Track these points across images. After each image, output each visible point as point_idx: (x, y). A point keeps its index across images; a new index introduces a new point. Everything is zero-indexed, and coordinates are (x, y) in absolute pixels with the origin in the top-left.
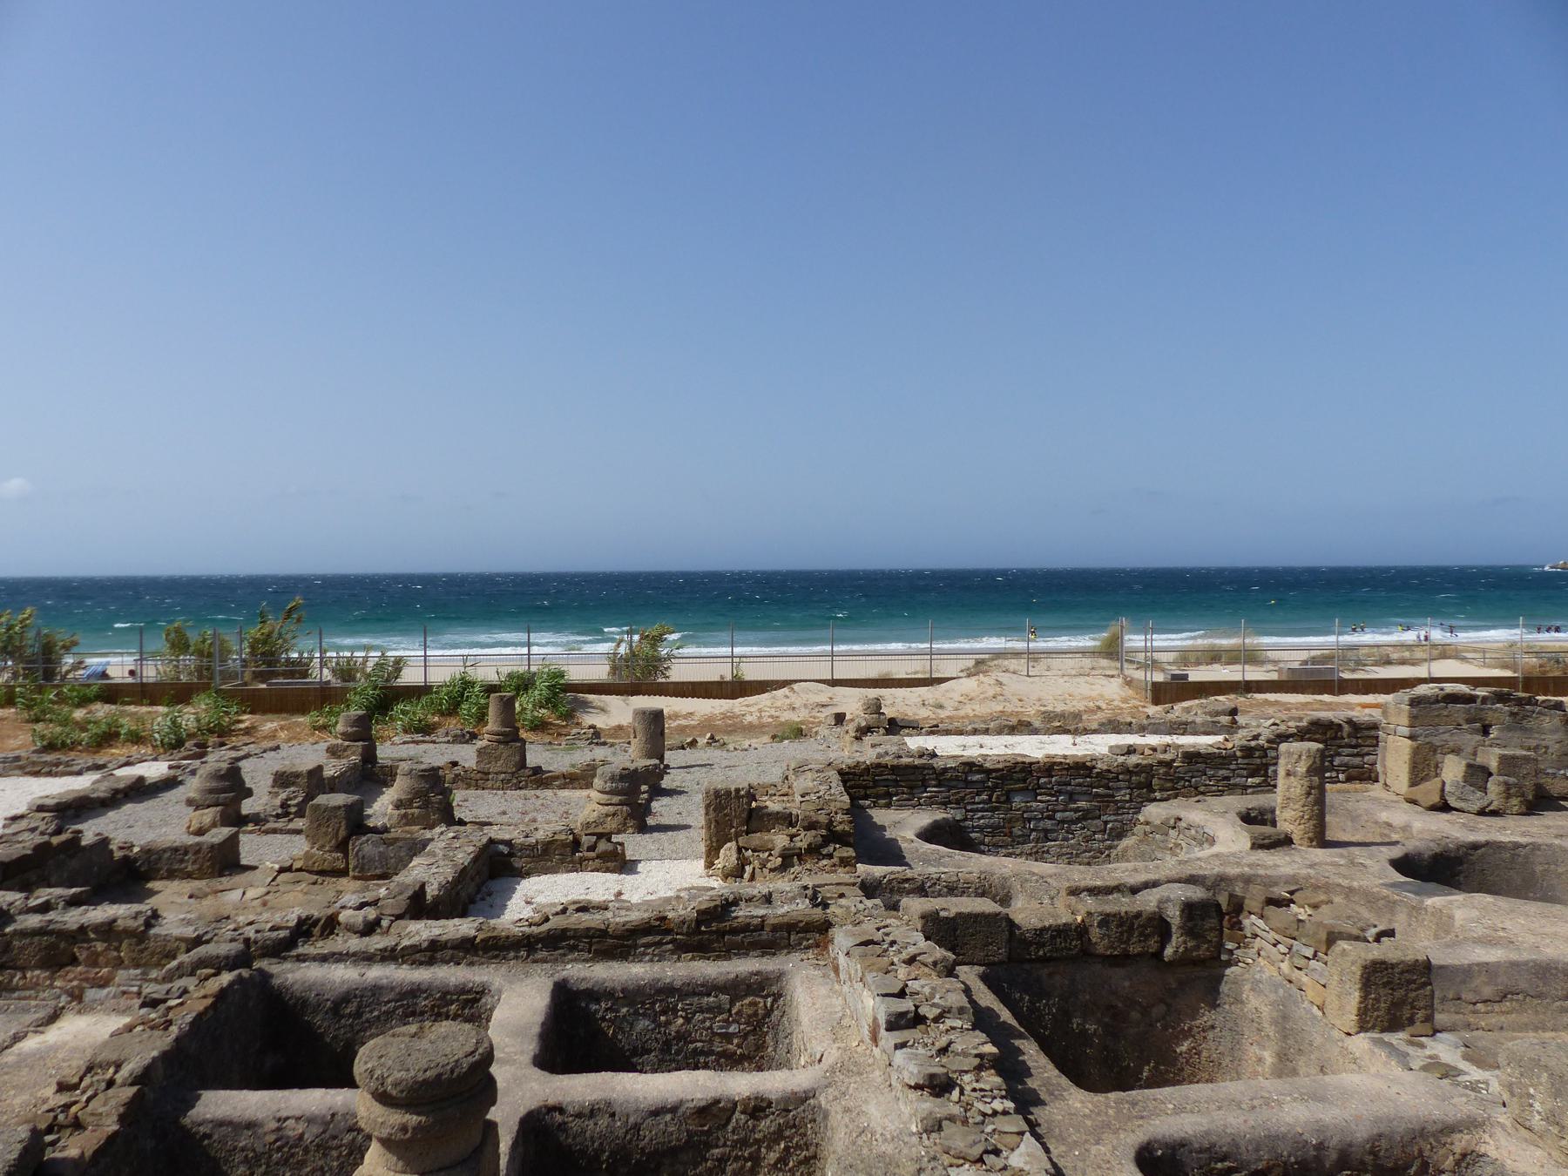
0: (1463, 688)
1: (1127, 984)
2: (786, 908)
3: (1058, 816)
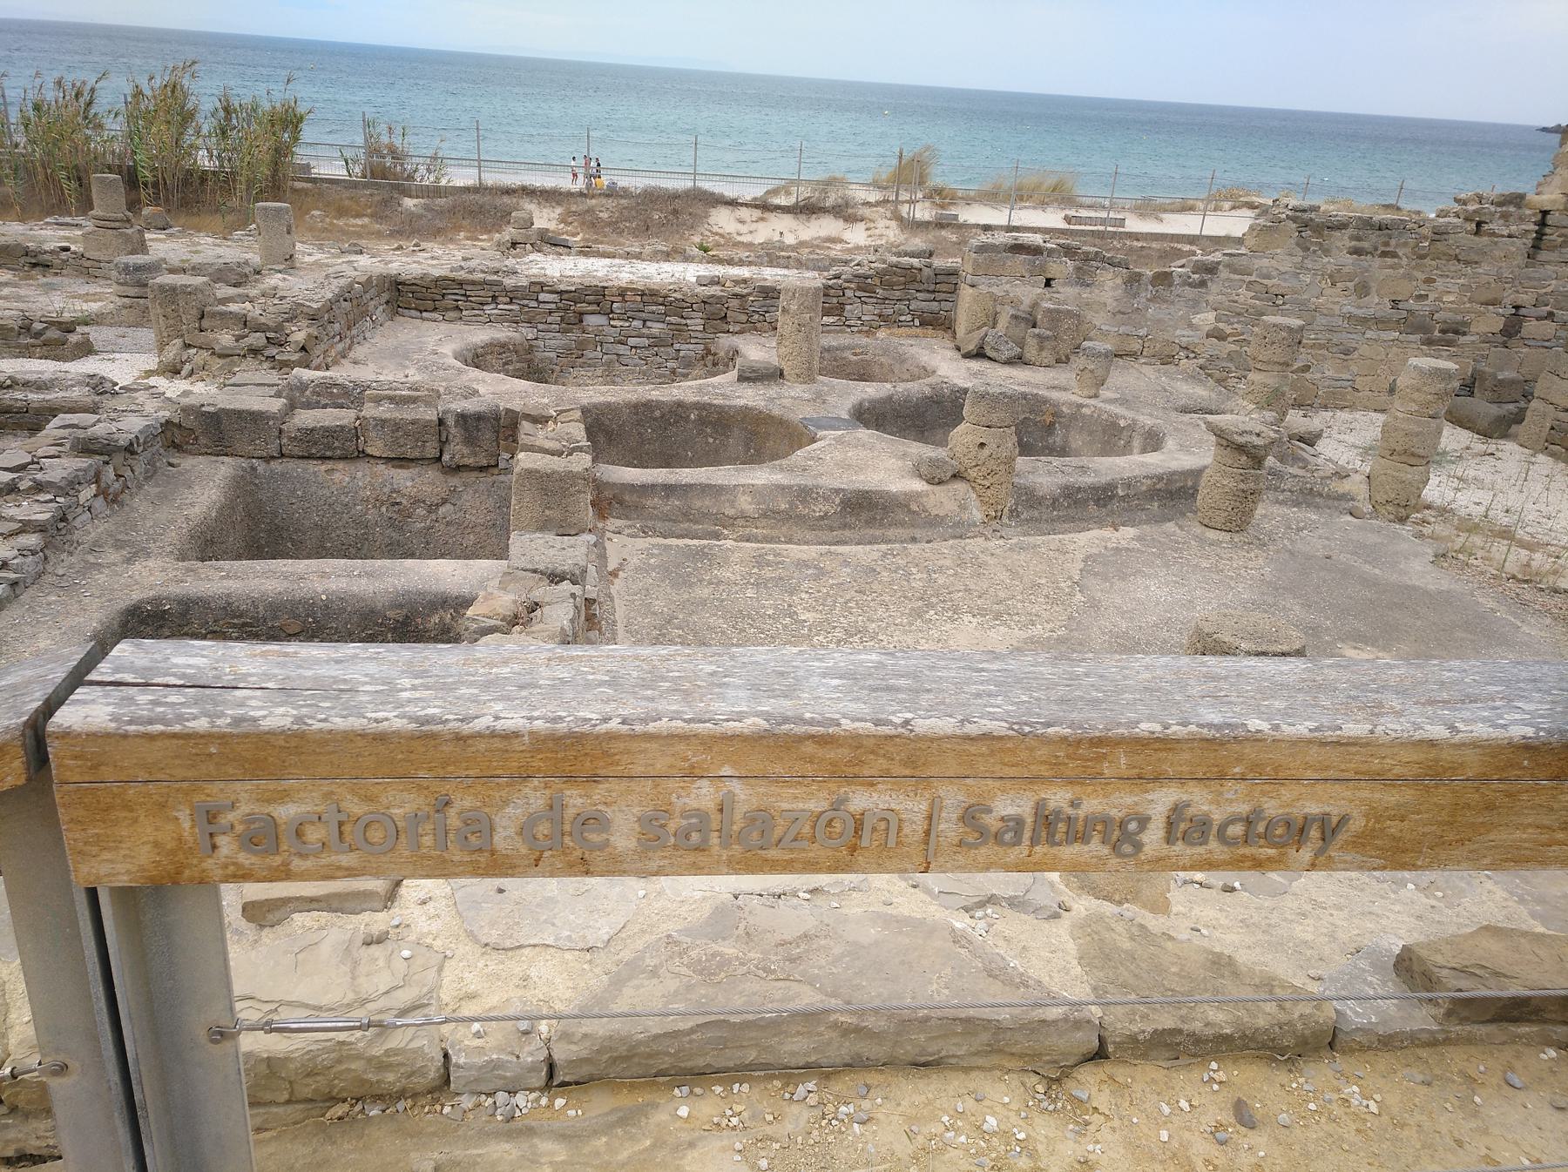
0: (1037, 239)
1: (409, 484)
2: (61, 394)
3: (632, 341)
